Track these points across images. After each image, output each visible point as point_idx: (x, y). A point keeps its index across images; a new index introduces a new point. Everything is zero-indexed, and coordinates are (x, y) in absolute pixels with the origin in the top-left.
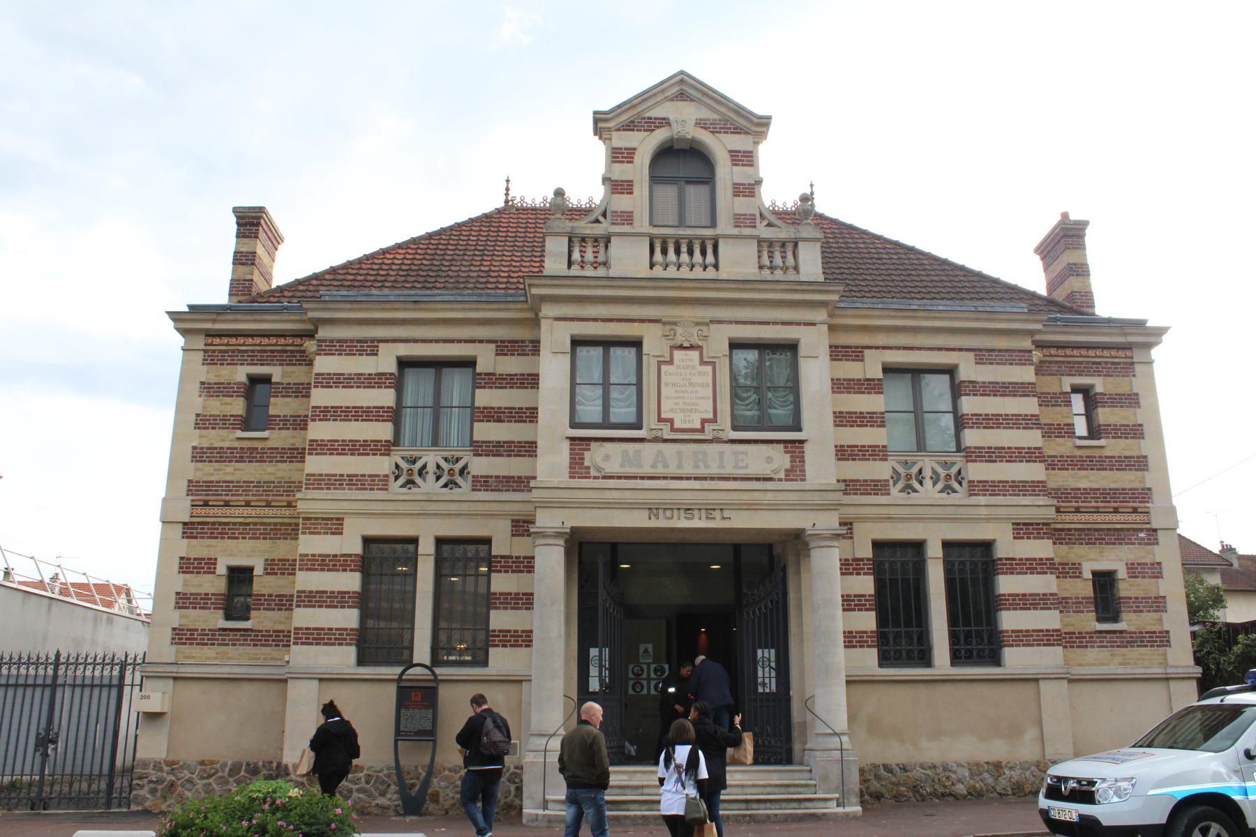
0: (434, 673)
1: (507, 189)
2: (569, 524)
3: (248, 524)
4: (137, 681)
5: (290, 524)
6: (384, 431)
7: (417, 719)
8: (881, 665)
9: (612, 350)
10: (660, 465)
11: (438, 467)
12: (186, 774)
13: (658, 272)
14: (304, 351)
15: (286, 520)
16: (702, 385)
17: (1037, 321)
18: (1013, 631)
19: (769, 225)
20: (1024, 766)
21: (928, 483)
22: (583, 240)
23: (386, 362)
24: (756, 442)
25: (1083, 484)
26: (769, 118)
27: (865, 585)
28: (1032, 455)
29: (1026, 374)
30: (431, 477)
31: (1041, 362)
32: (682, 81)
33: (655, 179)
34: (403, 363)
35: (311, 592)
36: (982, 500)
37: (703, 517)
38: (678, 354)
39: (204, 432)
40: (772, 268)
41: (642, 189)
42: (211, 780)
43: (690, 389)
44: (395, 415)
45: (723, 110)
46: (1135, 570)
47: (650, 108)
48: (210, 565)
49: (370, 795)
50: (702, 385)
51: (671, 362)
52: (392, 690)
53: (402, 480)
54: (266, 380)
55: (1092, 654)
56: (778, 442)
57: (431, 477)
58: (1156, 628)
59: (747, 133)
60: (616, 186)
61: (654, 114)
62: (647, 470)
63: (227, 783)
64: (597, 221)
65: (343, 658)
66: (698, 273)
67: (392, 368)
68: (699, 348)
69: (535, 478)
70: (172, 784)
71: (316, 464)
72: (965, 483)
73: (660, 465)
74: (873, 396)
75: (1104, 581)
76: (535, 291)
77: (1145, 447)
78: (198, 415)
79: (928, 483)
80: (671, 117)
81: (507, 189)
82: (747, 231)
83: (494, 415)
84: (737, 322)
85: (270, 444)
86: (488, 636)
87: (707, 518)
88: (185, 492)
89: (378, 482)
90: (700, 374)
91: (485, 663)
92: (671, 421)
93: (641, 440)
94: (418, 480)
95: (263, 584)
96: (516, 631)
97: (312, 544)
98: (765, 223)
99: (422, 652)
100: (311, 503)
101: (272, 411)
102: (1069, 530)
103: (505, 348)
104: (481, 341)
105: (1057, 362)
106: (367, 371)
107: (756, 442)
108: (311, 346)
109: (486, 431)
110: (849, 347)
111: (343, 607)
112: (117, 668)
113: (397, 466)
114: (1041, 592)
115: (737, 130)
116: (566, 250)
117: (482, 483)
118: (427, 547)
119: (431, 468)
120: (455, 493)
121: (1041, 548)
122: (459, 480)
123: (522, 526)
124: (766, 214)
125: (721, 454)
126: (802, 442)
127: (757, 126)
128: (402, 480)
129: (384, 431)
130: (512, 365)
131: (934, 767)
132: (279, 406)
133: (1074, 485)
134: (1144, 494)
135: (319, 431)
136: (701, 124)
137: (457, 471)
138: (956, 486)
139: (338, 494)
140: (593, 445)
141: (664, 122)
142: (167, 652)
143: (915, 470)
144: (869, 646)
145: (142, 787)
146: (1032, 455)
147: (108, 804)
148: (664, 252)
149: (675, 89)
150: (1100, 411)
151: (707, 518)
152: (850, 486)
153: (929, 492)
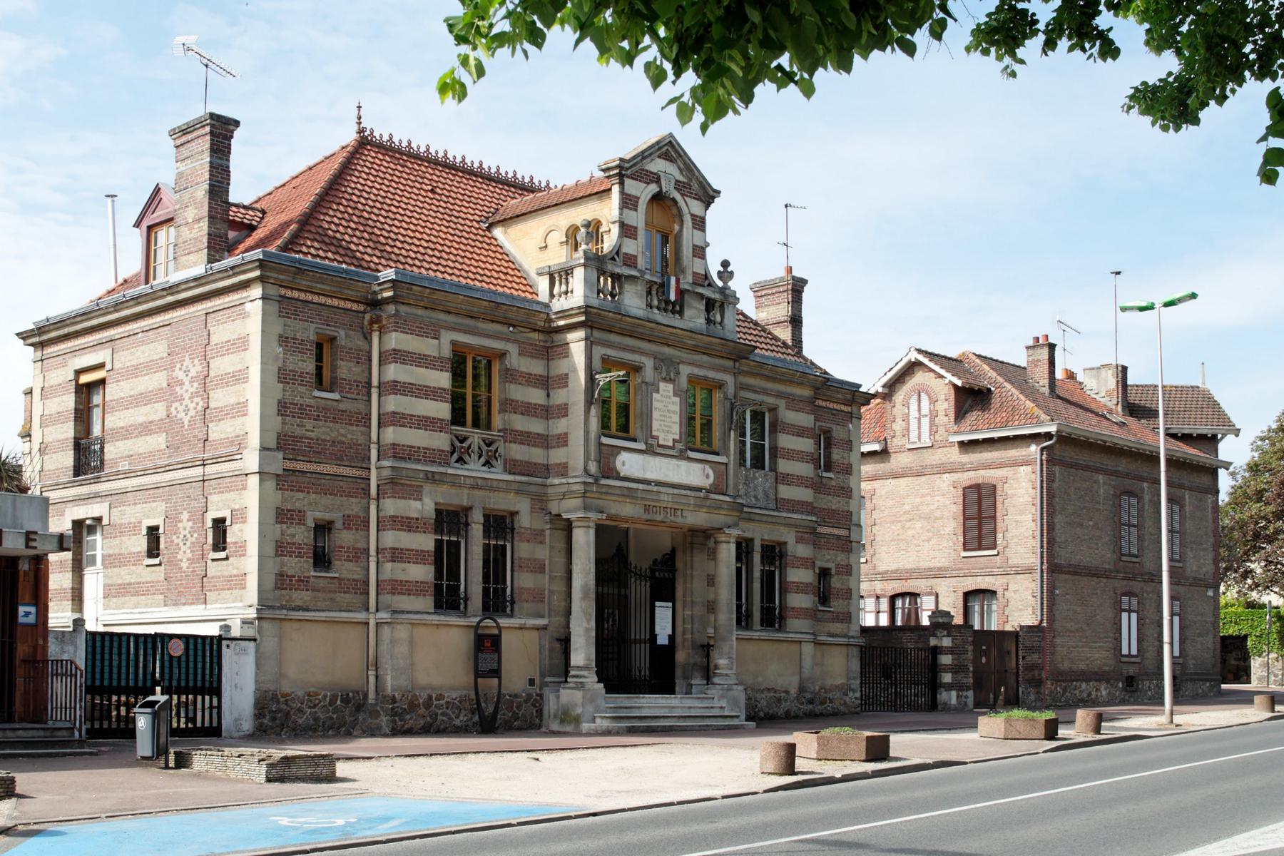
1: (359, 118)
7: (487, 661)
49: (450, 718)
53: (455, 456)
63: (328, 711)
75: (824, 574)
81: (359, 118)
127: (708, 196)
128: (455, 456)
141: (656, 179)
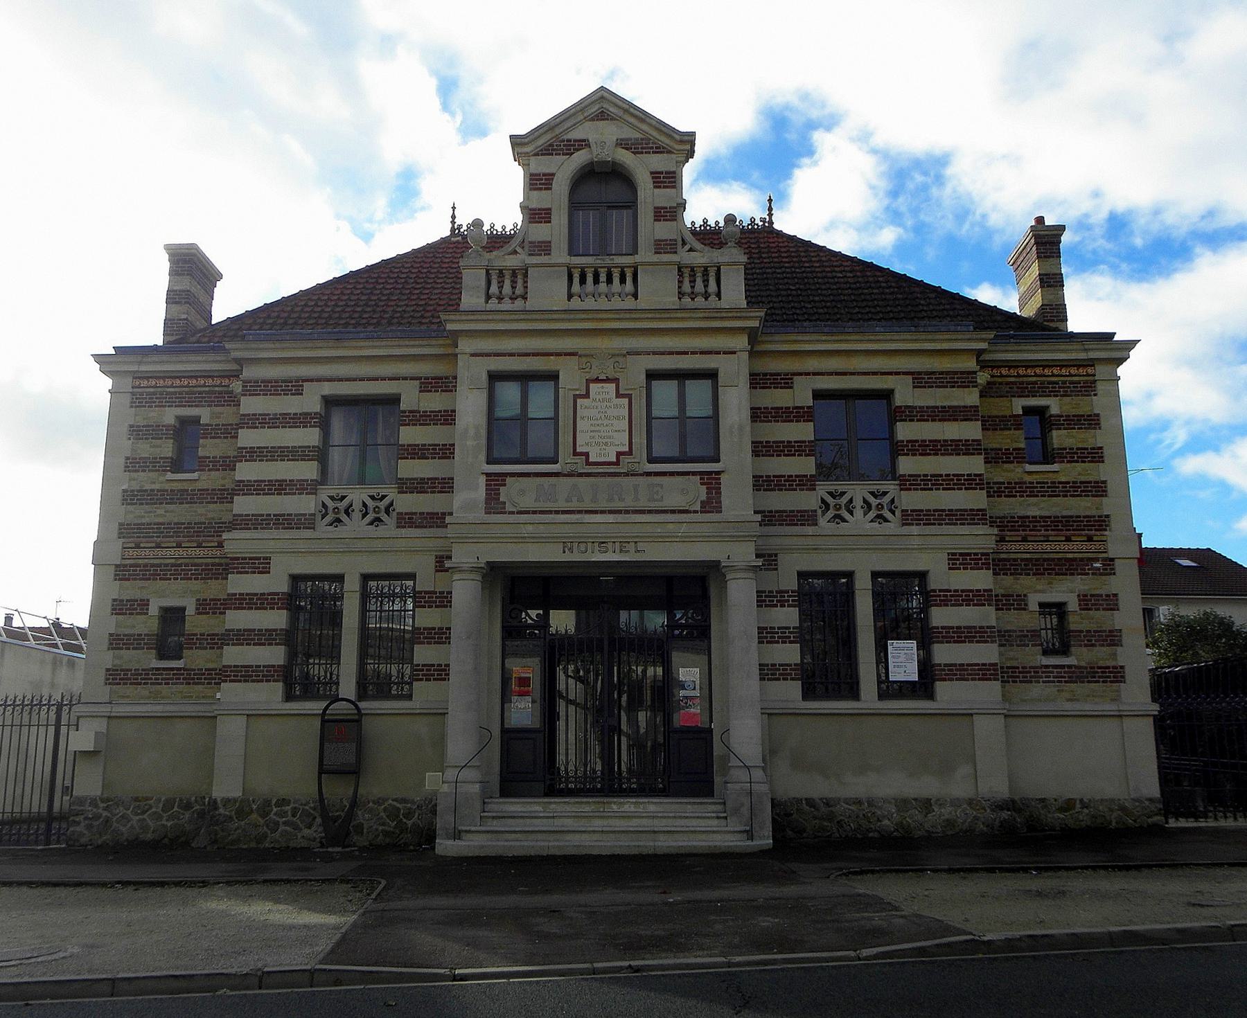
0: (356, 706)
2: (483, 560)
3: (180, 565)
4: (73, 721)
5: (220, 565)
6: (309, 470)
8: (806, 697)
9: (531, 384)
10: (574, 499)
11: (365, 505)
12: (121, 810)
13: (576, 303)
14: (232, 392)
15: (217, 561)
16: (618, 418)
17: (983, 340)
18: (946, 665)
19: (691, 250)
20: (956, 803)
21: (859, 512)
22: (501, 273)
23: (310, 402)
24: (672, 474)
25: (1033, 512)
26: (693, 134)
27: (788, 616)
28: (970, 482)
29: (970, 397)
30: (356, 515)
31: (989, 383)
32: (602, 97)
33: (575, 205)
34: (330, 402)
35: (239, 630)
36: (915, 529)
37: (618, 551)
38: (594, 387)
39: (135, 475)
40: (693, 296)
41: (560, 219)
42: (145, 816)
43: (606, 422)
44: (321, 455)
45: (645, 127)
46: (1087, 602)
47: (567, 130)
48: (144, 604)
49: (296, 828)
50: (618, 418)
51: (587, 396)
52: (317, 723)
53: (329, 518)
54: (196, 420)
55: (1036, 689)
56: (694, 473)
57: (356, 515)
58: (1111, 663)
59: (669, 152)
60: (534, 214)
61: (576, 135)
62: (562, 504)
64: (515, 252)
65: (269, 695)
66: (617, 303)
67: (316, 406)
68: (615, 380)
69: (451, 514)
70: (107, 821)
71: (244, 505)
72: (898, 513)
73: (574, 499)
74: (801, 424)
76: (449, 327)
77: (1102, 472)
78: (127, 458)
79: (859, 512)
80: (592, 138)
82: (666, 258)
83: (417, 452)
84: (655, 353)
85: (199, 485)
86: (413, 670)
87: (621, 551)
88: (116, 535)
89: (307, 522)
90: (616, 406)
91: (409, 697)
92: (587, 455)
93: (557, 474)
94: (344, 517)
95: (195, 623)
96: (440, 665)
97: (241, 583)
98: (687, 247)
99: (348, 688)
100: (238, 543)
101: (201, 453)
102: (1015, 560)
103: (430, 384)
104: (405, 379)
105: (1007, 383)
106: (292, 411)
107: (672, 474)
108: (237, 386)
109: (411, 469)
110: (779, 374)
111: (270, 644)
112: (54, 708)
113: (324, 505)
114: (977, 624)
115: (659, 150)
116: (483, 283)
117: (407, 520)
118: (352, 585)
119: (357, 506)
120: (381, 531)
121: (981, 580)
122: (384, 517)
123: (442, 564)
124: (689, 237)
125: (636, 487)
126: (718, 473)
128: (329, 518)
129: (309, 470)
130: (434, 402)
131: (859, 802)
132: (209, 448)
133: (1022, 513)
134: (1101, 523)
135: (247, 471)
136: (623, 144)
137: (383, 508)
138: (888, 515)
139: (266, 534)
140: (508, 480)
141: (583, 144)
142: (104, 693)
143: (844, 500)
144: (792, 679)
145: (78, 823)
146: (970, 482)
147: (48, 842)
148: (583, 281)
149: (597, 107)
150: (1055, 433)
151: (621, 551)
152: (769, 518)
153: (859, 521)
